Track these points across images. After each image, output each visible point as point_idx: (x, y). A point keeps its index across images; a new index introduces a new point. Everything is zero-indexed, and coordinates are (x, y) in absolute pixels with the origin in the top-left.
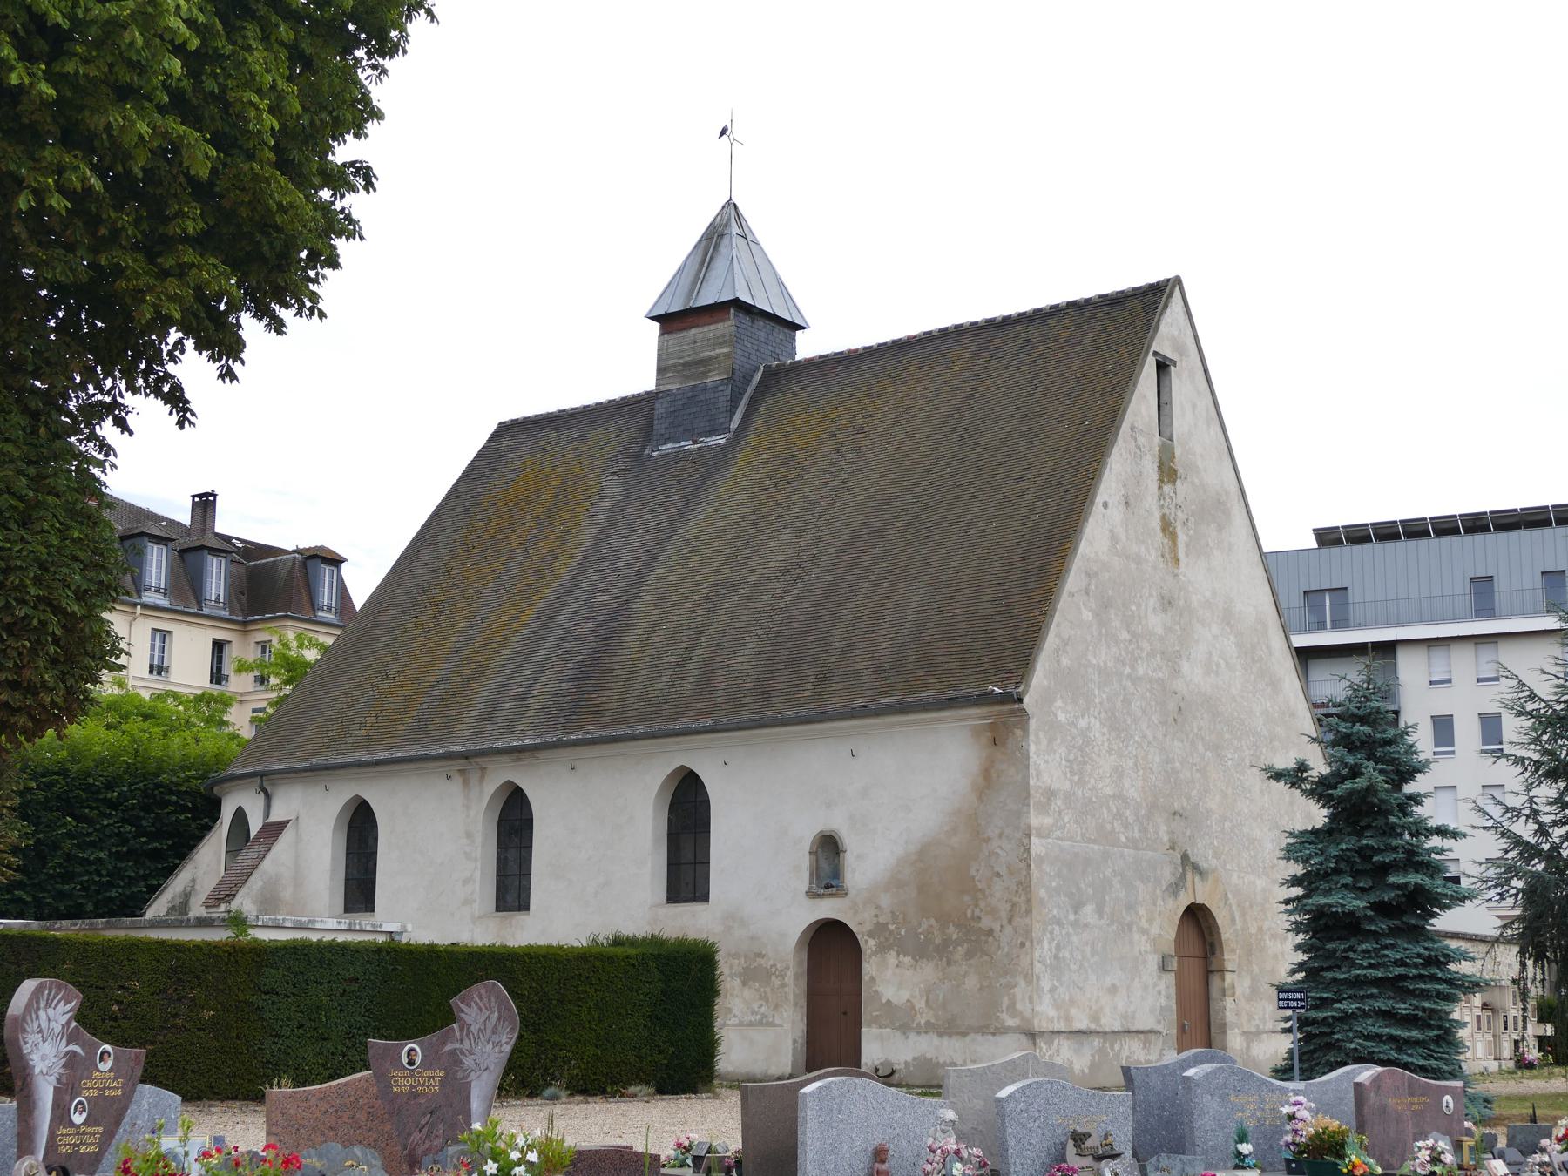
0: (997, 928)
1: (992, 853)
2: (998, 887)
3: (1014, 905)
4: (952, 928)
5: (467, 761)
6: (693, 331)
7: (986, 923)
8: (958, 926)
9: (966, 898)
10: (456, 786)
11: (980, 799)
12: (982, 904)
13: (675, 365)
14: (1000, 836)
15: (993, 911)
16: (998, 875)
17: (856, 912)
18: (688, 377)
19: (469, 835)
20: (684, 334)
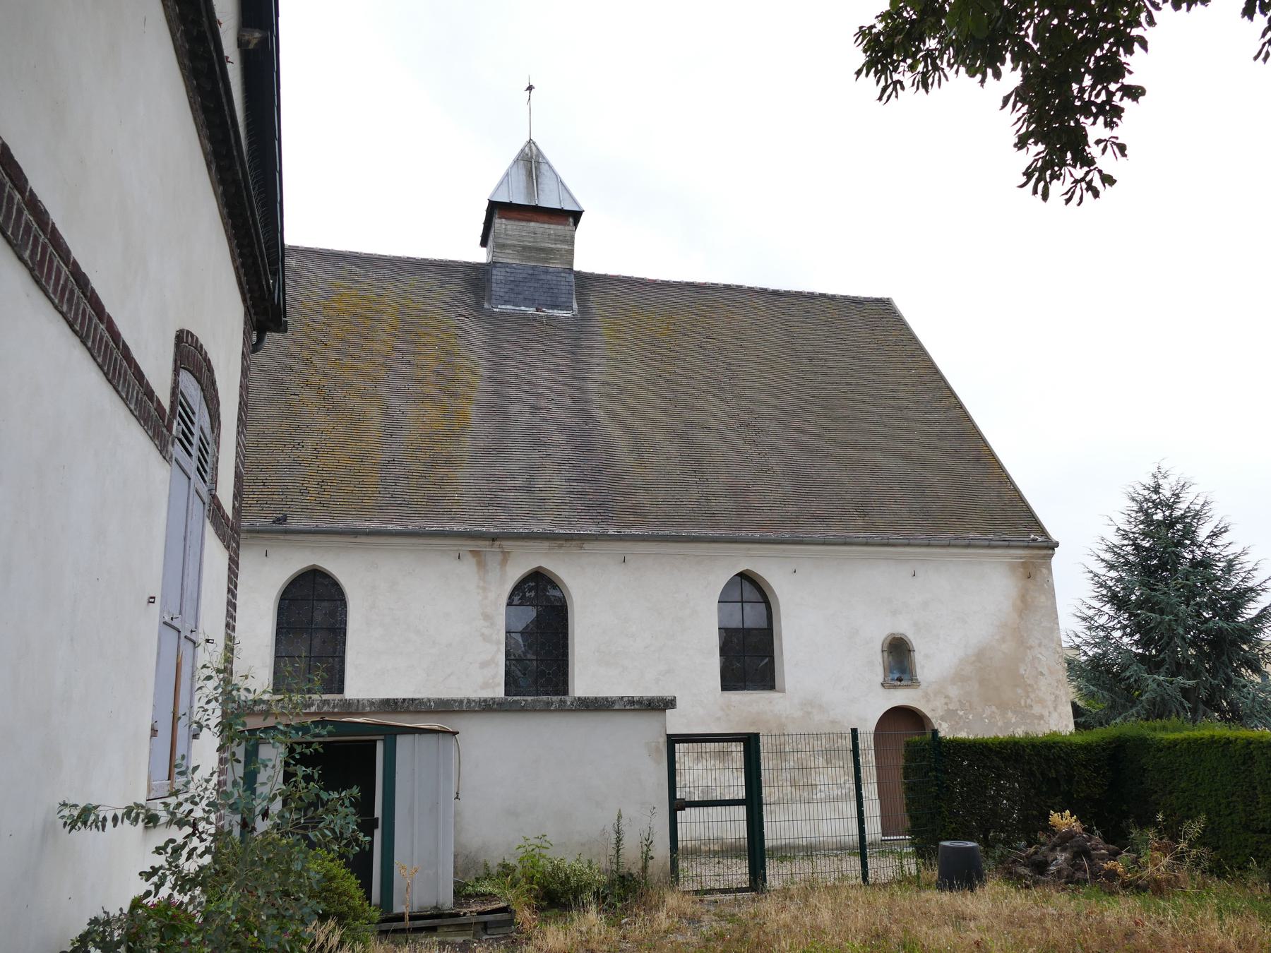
0: (1046, 713)
1: (1034, 658)
2: (1043, 683)
3: (1057, 697)
4: (1010, 714)
5: (486, 541)
6: (532, 224)
7: (1037, 710)
8: (1015, 712)
9: (1019, 691)
10: (468, 567)
11: (1020, 616)
12: (1032, 696)
13: (514, 246)
14: (1040, 645)
15: (1041, 701)
16: (1042, 674)
17: (928, 701)
18: (529, 258)
19: (486, 617)
20: (524, 224)
